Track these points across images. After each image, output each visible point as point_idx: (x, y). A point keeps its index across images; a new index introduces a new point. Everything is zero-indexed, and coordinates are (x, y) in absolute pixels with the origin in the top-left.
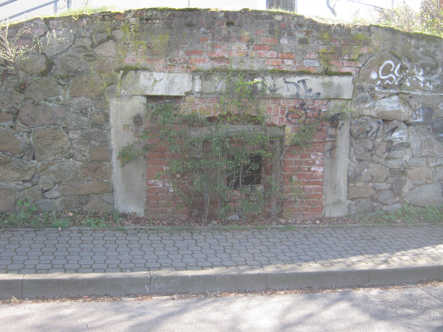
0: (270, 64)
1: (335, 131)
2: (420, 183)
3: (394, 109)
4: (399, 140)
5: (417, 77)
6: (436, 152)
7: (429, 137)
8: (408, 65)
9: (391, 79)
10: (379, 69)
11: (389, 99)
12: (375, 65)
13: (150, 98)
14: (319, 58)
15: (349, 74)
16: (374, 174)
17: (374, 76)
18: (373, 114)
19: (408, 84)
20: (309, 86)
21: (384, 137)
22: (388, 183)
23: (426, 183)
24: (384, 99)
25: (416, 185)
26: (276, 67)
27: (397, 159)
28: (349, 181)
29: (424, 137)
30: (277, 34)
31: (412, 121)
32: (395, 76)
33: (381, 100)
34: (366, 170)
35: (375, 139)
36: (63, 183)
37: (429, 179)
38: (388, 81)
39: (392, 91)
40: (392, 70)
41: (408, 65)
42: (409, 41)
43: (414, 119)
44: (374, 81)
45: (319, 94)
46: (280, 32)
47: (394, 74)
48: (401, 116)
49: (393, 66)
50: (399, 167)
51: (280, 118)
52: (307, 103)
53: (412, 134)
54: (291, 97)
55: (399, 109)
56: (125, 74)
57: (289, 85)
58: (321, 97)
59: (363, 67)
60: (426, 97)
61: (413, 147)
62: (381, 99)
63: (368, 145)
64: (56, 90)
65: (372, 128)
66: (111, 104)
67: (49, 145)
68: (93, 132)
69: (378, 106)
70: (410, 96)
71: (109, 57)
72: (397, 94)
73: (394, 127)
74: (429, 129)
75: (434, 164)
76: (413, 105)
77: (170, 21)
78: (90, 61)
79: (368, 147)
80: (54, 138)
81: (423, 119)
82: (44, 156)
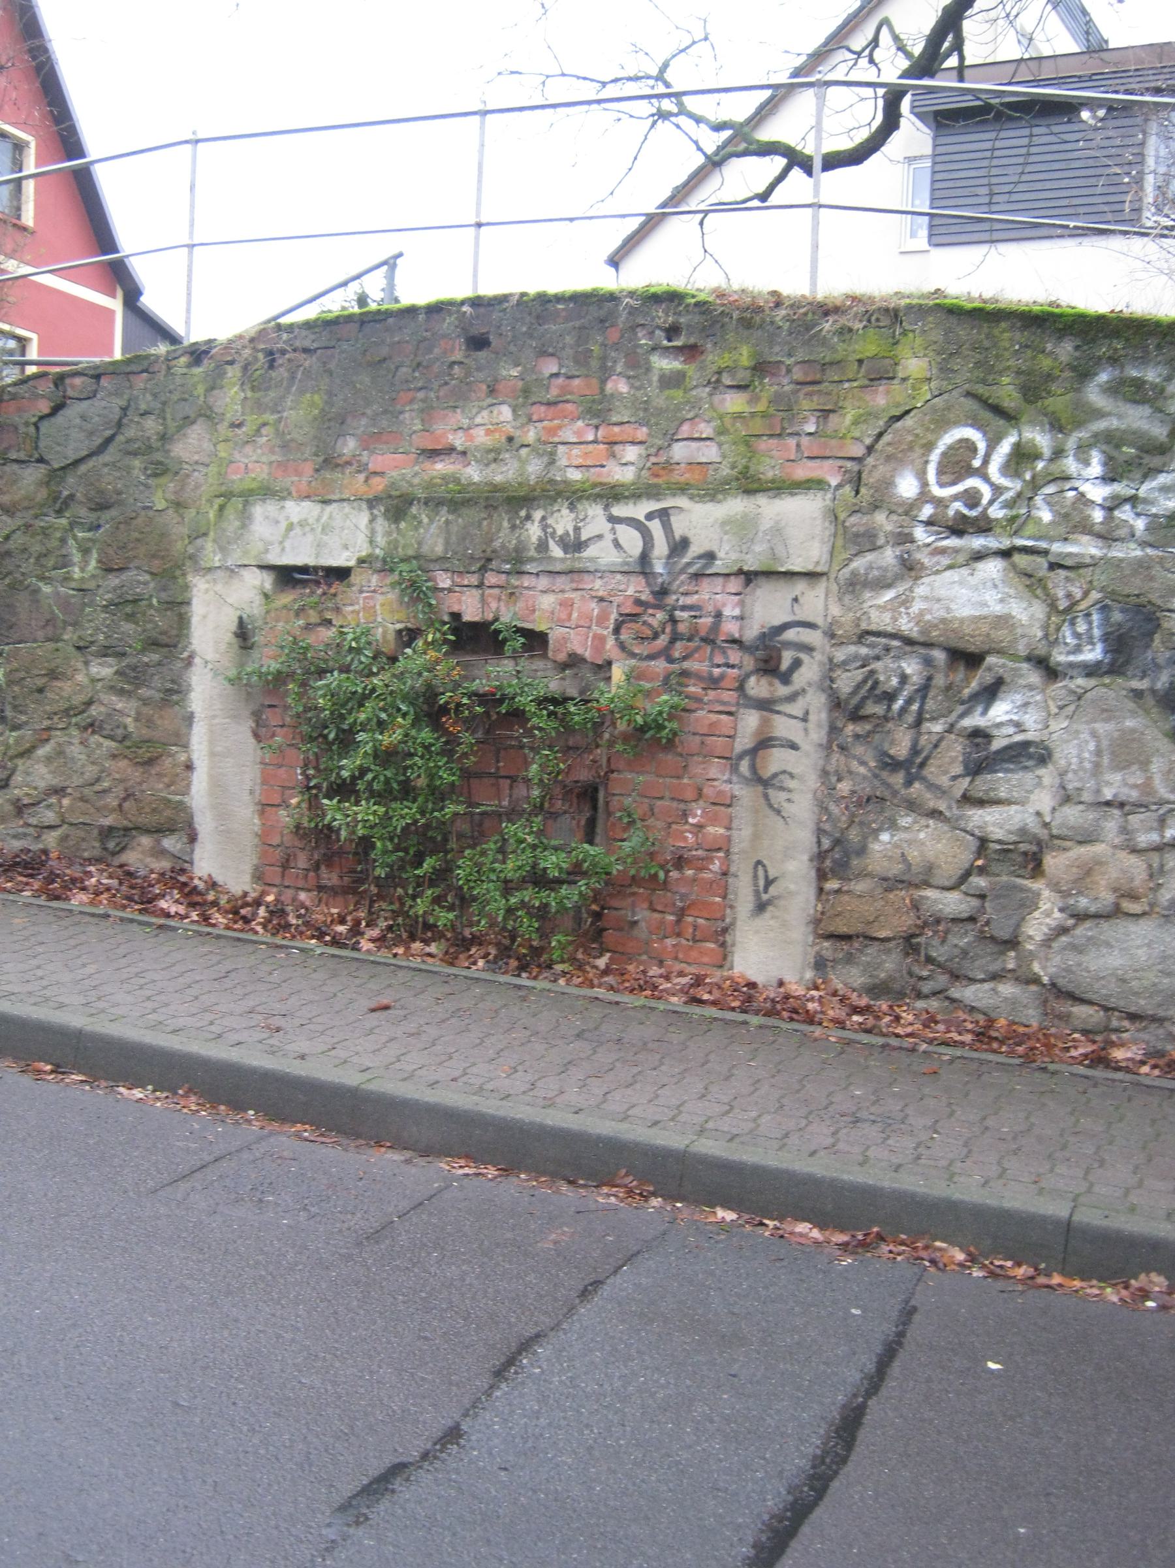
0: (576, 463)
1: (771, 684)
2: (1093, 910)
3: (985, 611)
4: (1011, 730)
5: (1076, 484)
6: (1157, 782)
7: (1129, 723)
8: (1042, 440)
9: (971, 497)
10: (927, 462)
11: (965, 571)
12: (911, 448)
13: (288, 576)
14: (720, 433)
15: (816, 484)
16: (913, 855)
17: (907, 487)
18: (906, 625)
19: (1046, 516)
20: (680, 527)
21: (954, 715)
22: (966, 894)
23: (1115, 912)
24: (948, 573)
25: (1081, 917)
26: (592, 470)
27: (1008, 802)
28: (822, 876)
29: (1110, 727)
30: (594, 364)
31: (1062, 658)
32: (992, 484)
33: (938, 577)
34: (885, 837)
35: (918, 722)
36: (69, 790)
37: (1133, 897)
38: (958, 506)
39: (978, 542)
40: (977, 463)
41: (1042, 440)
42: (1049, 346)
43: (1069, 653)
44: (909, 509)
45: (710, 556)
46: (604, 359)
47: (986, 478)
48: (1015, 641)
49: (982, 446)
50: (1014, 838)
51: (595, 636)
52: (674, 587)
53: (1061, 708)
54: (626, 568)
55: (1006, 611)
56: (222, 508)
57: (621, 528)
58: (718, 566)
59: (870, 461)
60: (1118, 564)
61: (1063, 762)
62: (938, 572)
63: (892, 742)
64: (64, 552)
65: (904, 678)
66: (195, 591)
67: (40, 691)
68: (147, 665)
69: (926, 598)
70: (1051, 558)
71: (196, 463)
72: (1006, 554)
73: (989, 679)
74: (1138, 694)
75: (1154, 837)
76: (1061, 594)
77: (329, 352)
78: (155, 475)
79: (892, 752)
80: (53, 675)
81: (1106, 652)
82: (24, 718)
